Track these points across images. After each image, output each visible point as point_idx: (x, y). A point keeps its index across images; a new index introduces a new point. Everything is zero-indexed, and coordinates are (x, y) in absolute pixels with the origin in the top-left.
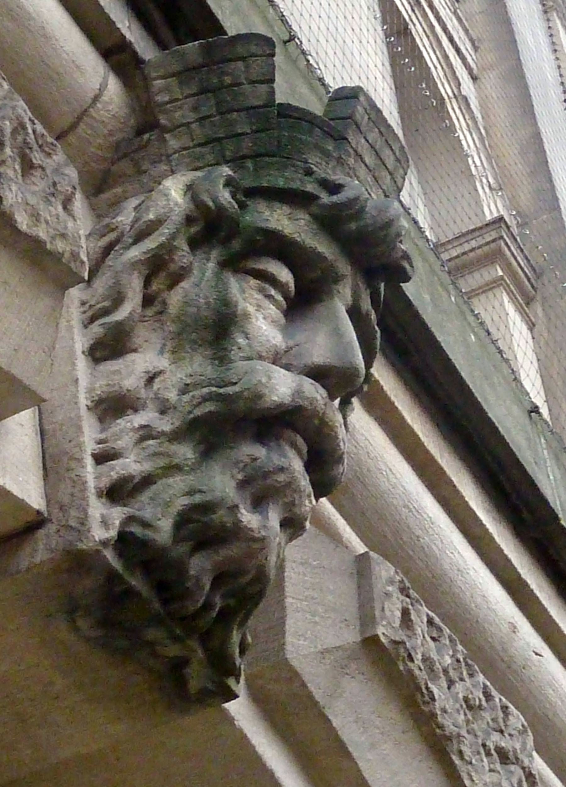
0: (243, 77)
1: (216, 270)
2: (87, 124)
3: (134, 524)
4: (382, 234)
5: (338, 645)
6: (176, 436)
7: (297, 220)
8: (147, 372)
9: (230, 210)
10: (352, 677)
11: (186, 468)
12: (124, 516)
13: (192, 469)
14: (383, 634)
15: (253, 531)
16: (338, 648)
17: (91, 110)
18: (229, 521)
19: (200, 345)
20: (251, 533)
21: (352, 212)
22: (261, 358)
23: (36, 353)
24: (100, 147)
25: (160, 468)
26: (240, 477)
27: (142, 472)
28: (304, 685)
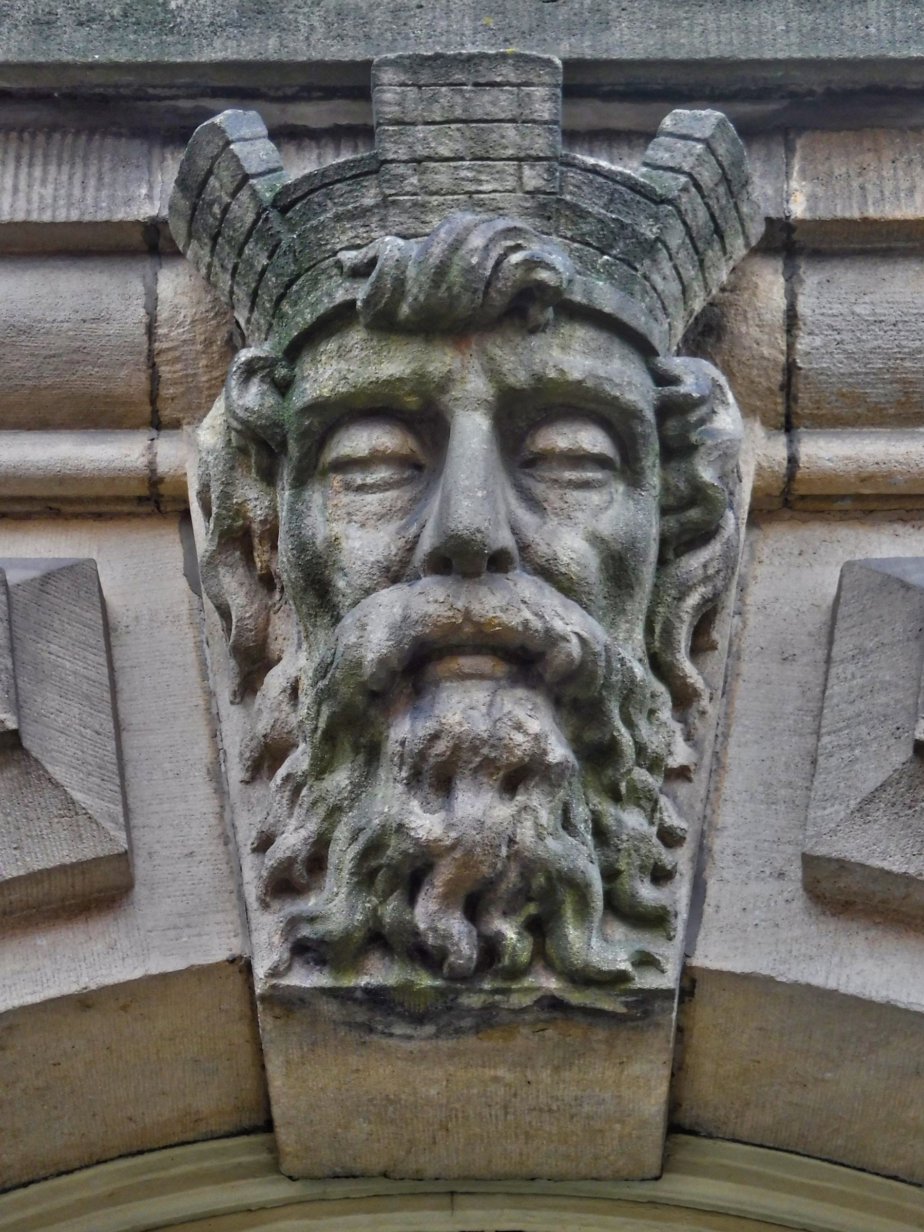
1: (451, 387)
2: (168, 362)
3: (302, 926)
4: (442, 293)
5: (879, 784)
6: (322, 767)
8: (284, 691)
9: (251, 419)
12: (282, 925)
13: (353, 800)
15: (440, 840)
16: (882, 787)
17: (157, 344)
19: (316, 616)
20: (442, 843)
22: (368, 592)
25: (324, 820)
26: (404, 774)
27: (310, 837)
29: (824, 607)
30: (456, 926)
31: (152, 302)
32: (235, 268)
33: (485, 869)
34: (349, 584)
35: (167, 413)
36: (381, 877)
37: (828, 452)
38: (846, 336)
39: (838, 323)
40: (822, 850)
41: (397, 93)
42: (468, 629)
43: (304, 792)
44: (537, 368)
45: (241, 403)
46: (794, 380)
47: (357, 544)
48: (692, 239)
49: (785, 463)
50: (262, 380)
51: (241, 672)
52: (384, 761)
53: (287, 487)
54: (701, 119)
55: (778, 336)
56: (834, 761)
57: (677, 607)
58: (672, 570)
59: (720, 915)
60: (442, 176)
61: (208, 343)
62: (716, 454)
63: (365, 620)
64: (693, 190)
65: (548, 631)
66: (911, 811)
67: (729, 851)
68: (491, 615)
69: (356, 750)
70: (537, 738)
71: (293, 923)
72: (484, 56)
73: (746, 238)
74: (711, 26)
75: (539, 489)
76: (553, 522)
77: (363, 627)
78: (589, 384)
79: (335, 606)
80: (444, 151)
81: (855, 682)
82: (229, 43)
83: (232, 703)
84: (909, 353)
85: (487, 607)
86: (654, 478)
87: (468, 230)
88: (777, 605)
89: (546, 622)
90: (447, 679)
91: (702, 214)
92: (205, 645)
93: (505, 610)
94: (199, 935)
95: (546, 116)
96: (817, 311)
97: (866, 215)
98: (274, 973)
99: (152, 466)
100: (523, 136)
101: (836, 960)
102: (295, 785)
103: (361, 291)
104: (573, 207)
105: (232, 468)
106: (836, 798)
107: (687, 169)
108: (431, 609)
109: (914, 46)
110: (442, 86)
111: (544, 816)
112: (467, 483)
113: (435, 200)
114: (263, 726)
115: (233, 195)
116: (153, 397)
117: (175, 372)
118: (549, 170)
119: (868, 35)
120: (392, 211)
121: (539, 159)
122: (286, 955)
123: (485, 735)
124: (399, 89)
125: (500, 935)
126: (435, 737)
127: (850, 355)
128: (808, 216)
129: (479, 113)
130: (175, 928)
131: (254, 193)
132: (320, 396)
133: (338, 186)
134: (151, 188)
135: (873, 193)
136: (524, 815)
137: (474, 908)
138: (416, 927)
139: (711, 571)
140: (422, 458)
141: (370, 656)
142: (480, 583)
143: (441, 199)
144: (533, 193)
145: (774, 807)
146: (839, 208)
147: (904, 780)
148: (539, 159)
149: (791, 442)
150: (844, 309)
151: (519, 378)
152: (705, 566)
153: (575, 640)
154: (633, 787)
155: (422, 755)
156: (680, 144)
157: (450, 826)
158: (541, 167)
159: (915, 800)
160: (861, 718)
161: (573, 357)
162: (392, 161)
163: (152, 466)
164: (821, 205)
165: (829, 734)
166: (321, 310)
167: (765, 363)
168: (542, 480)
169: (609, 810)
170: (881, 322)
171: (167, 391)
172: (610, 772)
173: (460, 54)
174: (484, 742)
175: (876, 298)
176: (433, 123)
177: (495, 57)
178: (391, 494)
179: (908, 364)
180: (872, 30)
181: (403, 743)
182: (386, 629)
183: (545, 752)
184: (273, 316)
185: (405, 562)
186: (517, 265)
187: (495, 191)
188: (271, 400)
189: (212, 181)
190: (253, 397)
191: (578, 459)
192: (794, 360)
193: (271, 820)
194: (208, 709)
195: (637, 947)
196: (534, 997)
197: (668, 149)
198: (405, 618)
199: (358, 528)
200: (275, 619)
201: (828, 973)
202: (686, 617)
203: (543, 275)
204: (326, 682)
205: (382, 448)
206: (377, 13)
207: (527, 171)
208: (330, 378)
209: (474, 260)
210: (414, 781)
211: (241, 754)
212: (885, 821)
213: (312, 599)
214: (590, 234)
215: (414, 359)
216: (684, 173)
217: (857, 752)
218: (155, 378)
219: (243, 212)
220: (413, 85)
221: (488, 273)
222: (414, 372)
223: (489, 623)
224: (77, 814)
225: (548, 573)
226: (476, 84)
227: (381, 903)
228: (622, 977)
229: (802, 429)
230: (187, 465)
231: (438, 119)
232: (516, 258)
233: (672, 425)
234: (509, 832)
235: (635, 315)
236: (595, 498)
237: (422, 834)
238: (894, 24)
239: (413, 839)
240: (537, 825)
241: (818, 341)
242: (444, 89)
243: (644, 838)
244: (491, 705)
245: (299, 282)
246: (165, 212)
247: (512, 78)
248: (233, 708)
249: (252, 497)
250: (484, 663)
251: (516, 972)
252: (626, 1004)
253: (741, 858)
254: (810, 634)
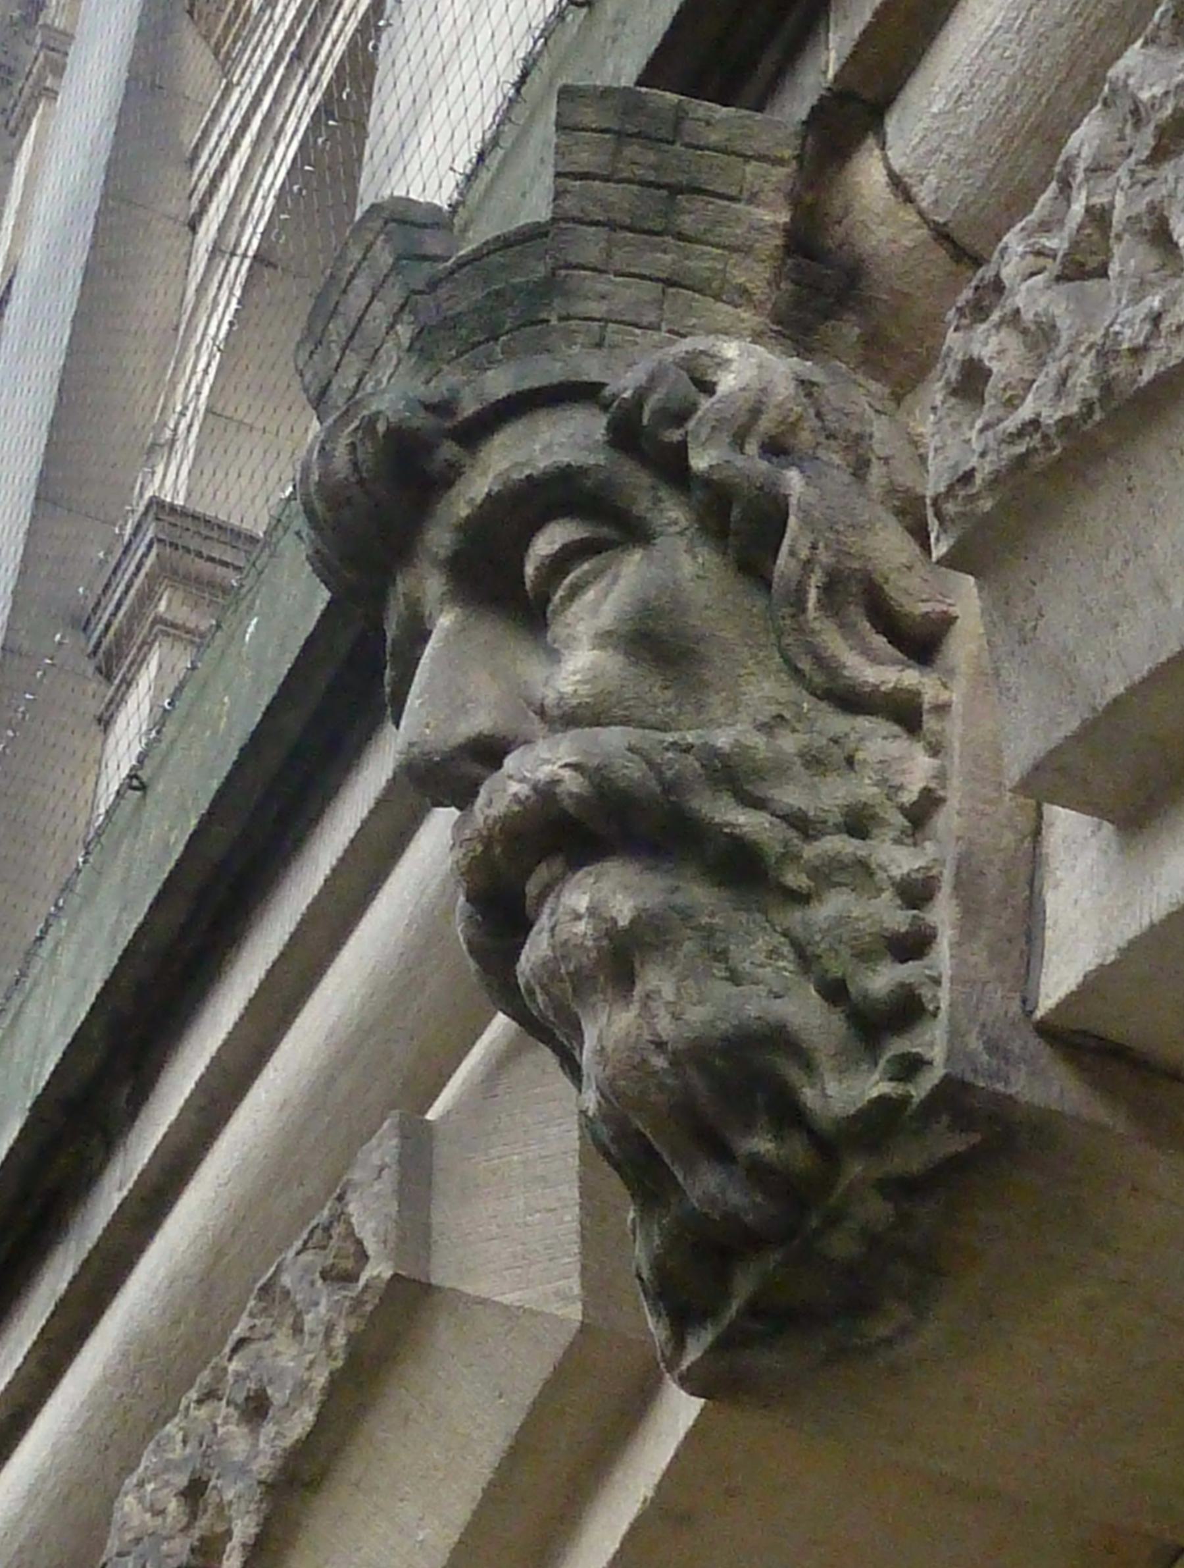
38: (947, 147)
55: (901, 214)
70: (592, 911)
127: (967, 162)
139: (804, 554)
167: (917, 254)
241: (932, 180)
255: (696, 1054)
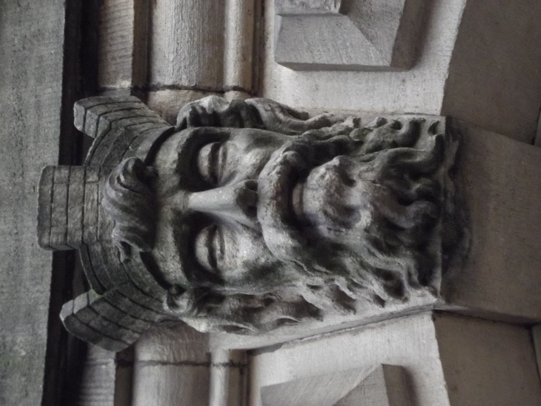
0: (98, 319)
4: (134, 209)
6: (343, 271)
7: (163, 256)
8: (313, 292)
9: (192, 303)
10: (371, 5)
11: (358, 259)
13: (357, 256)
14: (335, 6)
16: (361, 30)
18: (375, 228)
19: (279, 275)
21: (136, 235)
22: (265, 247)
23: (369, 398)
24: (183, 338)
25: (367, 271)
26: (344, 230)
27: (376, 279)
28: (397, 39)
29: (297, 75)
30: (412, 209)
31: (152, 363)
32: (133, 317)
33: (386, 194)
34: (263, 256)
35: (202, 358)
36: (390, 242)
37: (232, 75)
38: (183, 65)
39: (177, 67)
40: (389, 57)
41: (53, 236)
42: (280, 199)
43: (355, 280)
44: (172, 172)
45: (186, 308)
46: (201, 88)
47: (245, 252)
48: (129, 117)
49: (236, 92)
50: (176, 299)
51: (308, 316)
52: (339, 241)
53: (223, 289)
54: (77, 112)
55: (181, 93)
56: (352, 56)
57: (284, 123)
58: (268, 125)
59: (419, 105)
60: (90, 216)
61: (172, 338)
62: (218, 104)
63: (276, 246)
64: (107, 115)
65: (281, 163)
66: (372, 17)
67: (393, 105)
68: (273, 187)
69: (335, 255)
70: (327, 169)
71: (412, 284)
72: (40, 199)
73: (136, 102)
74: (48, 119)
75: (226, 174)
76: (240, 168)
77: (279, 246)
78: (180, 150)
79: (273, 264)
80: (79, 215)
81: (321, 50)
82: (40, 327)
83: (322, 321)
84: (191, 38)
85: (269, 189)
86: (226, 129)
87: (108, 198)
88: (296, 95)
89: (277, 165)
90: (302, 210)
91: (119, 113)
92: (303, 340)
93: (271, 182)
94: (423, 335)
95: (67, 171)
96: (171, 76)
97: (131, 55)
98: (434, 293)
99: (225, 365)
100: (75, 181)
101: (440, 53)
102: (353, 285)
103: (137, 250)
104: (107, 160)
105: (216, 315)
106: (367, 52)
107: (96, 117)
108: (269, 213)
109: (60, 34)
110: (51, 216)
111: (364, 168)
112: (216, 198)
113: (100, 219)
114: (328, 302)
115: (97, 314)
116: (195, 364)
117: (184, 354)
118: (91, 169)
119: (55, 53)
120: (104, 238)
121: (85, 174)
122: (427, 288)
123: (325, 190)
124: (52, 235)
125: (418, 191)
126: (326, 213)
127: (191, 64)
128: (130, 79)
129: (64, 200)
130: (419, 346)
131: (97, 302)
132: (181, 269)
133: (93, 263)
134: (103, 364)
135: (123, 53)
136: (363, 177)
137: (405, 201)
138: (414, 227)
139: (269, 108)
140: (212, 226)
141: (290, 242)
142: (260, 193)
143: (100, 216)
144: (99, 177)
145: (376, 87)
146: (128, 67)
147: (359, 20)
148: (85, 174)
149: (228, 90)
150: (171, 65)
151: (175, 180)
152: (267, 110)
153: (286, 153)
154: (358, 136)
155: (334, 220)
156: (87, 121)
157: (365, 207)
158: (88, 174)
159: (367, 15)
160: (335, 44)
161: (169, 157)
162: (82, 238)
163: (225, 365)
164: (126, 74)
165: (342, 60)
166: (145, 269)
168: (222, 173)
169: (366, 146)
170: (177, 50)
171: (193, 358)
172: (349, 145)
173: (38, 209)
174: (328, 191)
175: (166, 52)
176: (67, 220)
177: (40, 193)
178: (225, 238)
179: (196, 39)
180: (53, 52)
181: (329, 229)
182: (279, 235)
183: (335, 166)
184: (152, 297)
185: (253, 230)
186: (125, 178)
187: (98, 193)
188: (185, 295)
189: (92, 324)
190: (184, 303)
191: (213, 157)
192: (192, 87)
193: (368, 297)
194: (329, 337)
195: (426, 132)
196: (449, 179)
197: (90, 127)
198: (274, 226)
199: (239, 252)
200: (284, 299)
201: (445, 56)
202: (289, 119)
203: (130, 167)
204: (303, 265)
205: (205, 242)
206: (34, 263)
207: (90, 180)
208: (174, 265)
209: (121, 195)
210: (348, 226)
211: (343, 315)
212: (376, 29)
213: (271, 276)
214: (119, 153)
215: (166, 226)
216: (99, 118)
217: (348, 44)
218: (187, 363)
219: (104, 309)
220: (50, 230)
221: (127, 190)
222: (171, 225)
223: (276, 188)
224: (363, 385)
225: (259, 168)
226: (52, 201)
227: (403, 244)
228: (439, 139)
229: (223, 87)
230: (225, 349)
231: (65, 218)
232: (122, 179)
233: (203, 121)
234: (369, 182)
235: (156, 135)
236: (231, 151)
237: (369, 220)
238: (51, 43)
239: (371, 225)
240: (367, 171)
241: (184, 76)
242: (53, 216)
243: (379, 132)
244: (313, 189)
245: (134, 281)
246: (113, 354)
247: (50, 186)
248: (324, 320)
249: (228, 306)
250: (296, 193)
251: (436, 185)
252: (454, 140)
253: (397, 99)
254: (307, 80)
255: (385, 175)
